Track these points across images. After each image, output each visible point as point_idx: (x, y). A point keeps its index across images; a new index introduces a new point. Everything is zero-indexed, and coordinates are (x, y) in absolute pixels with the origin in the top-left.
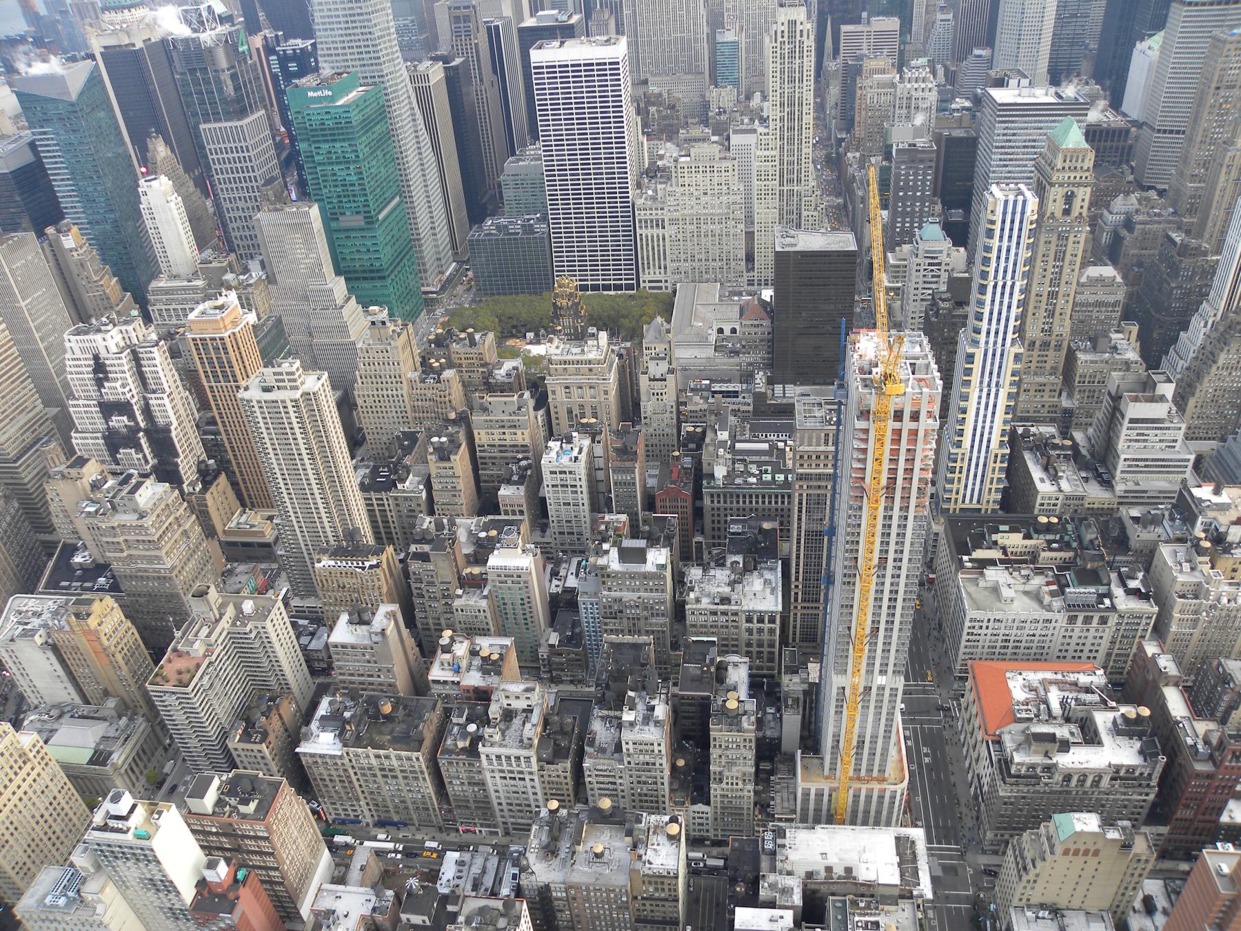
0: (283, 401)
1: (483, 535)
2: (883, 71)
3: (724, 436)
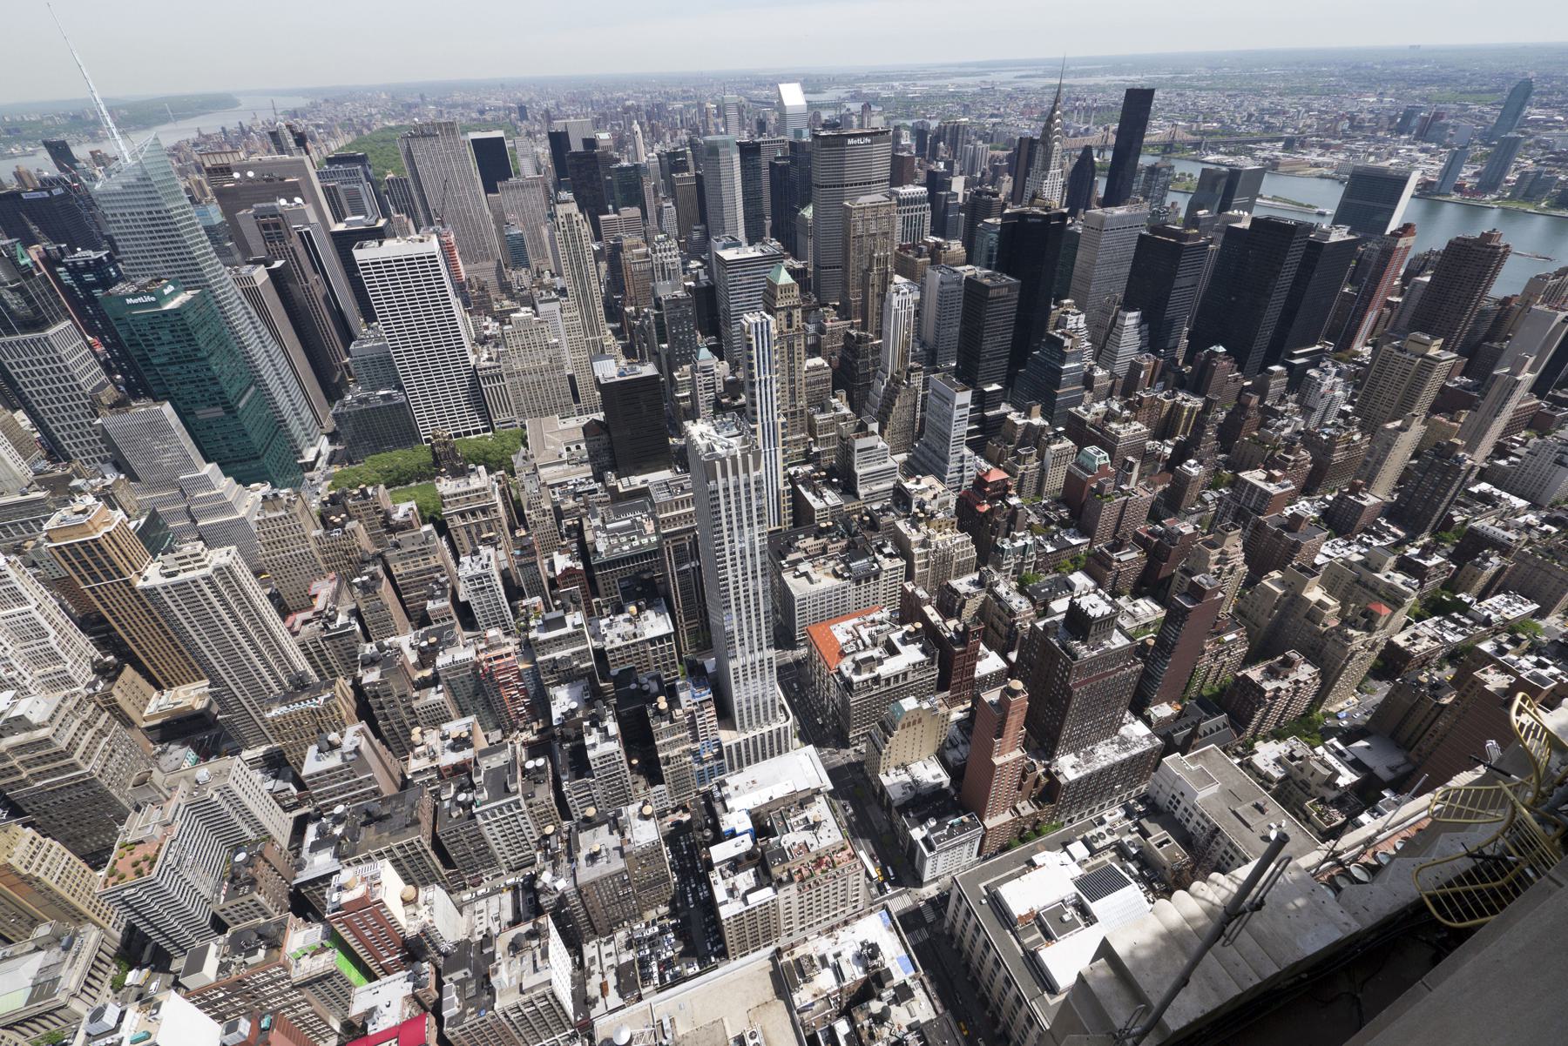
0: (193, 582)
1: (424, 644)
2: (638, 247)
3: (597, 522)
